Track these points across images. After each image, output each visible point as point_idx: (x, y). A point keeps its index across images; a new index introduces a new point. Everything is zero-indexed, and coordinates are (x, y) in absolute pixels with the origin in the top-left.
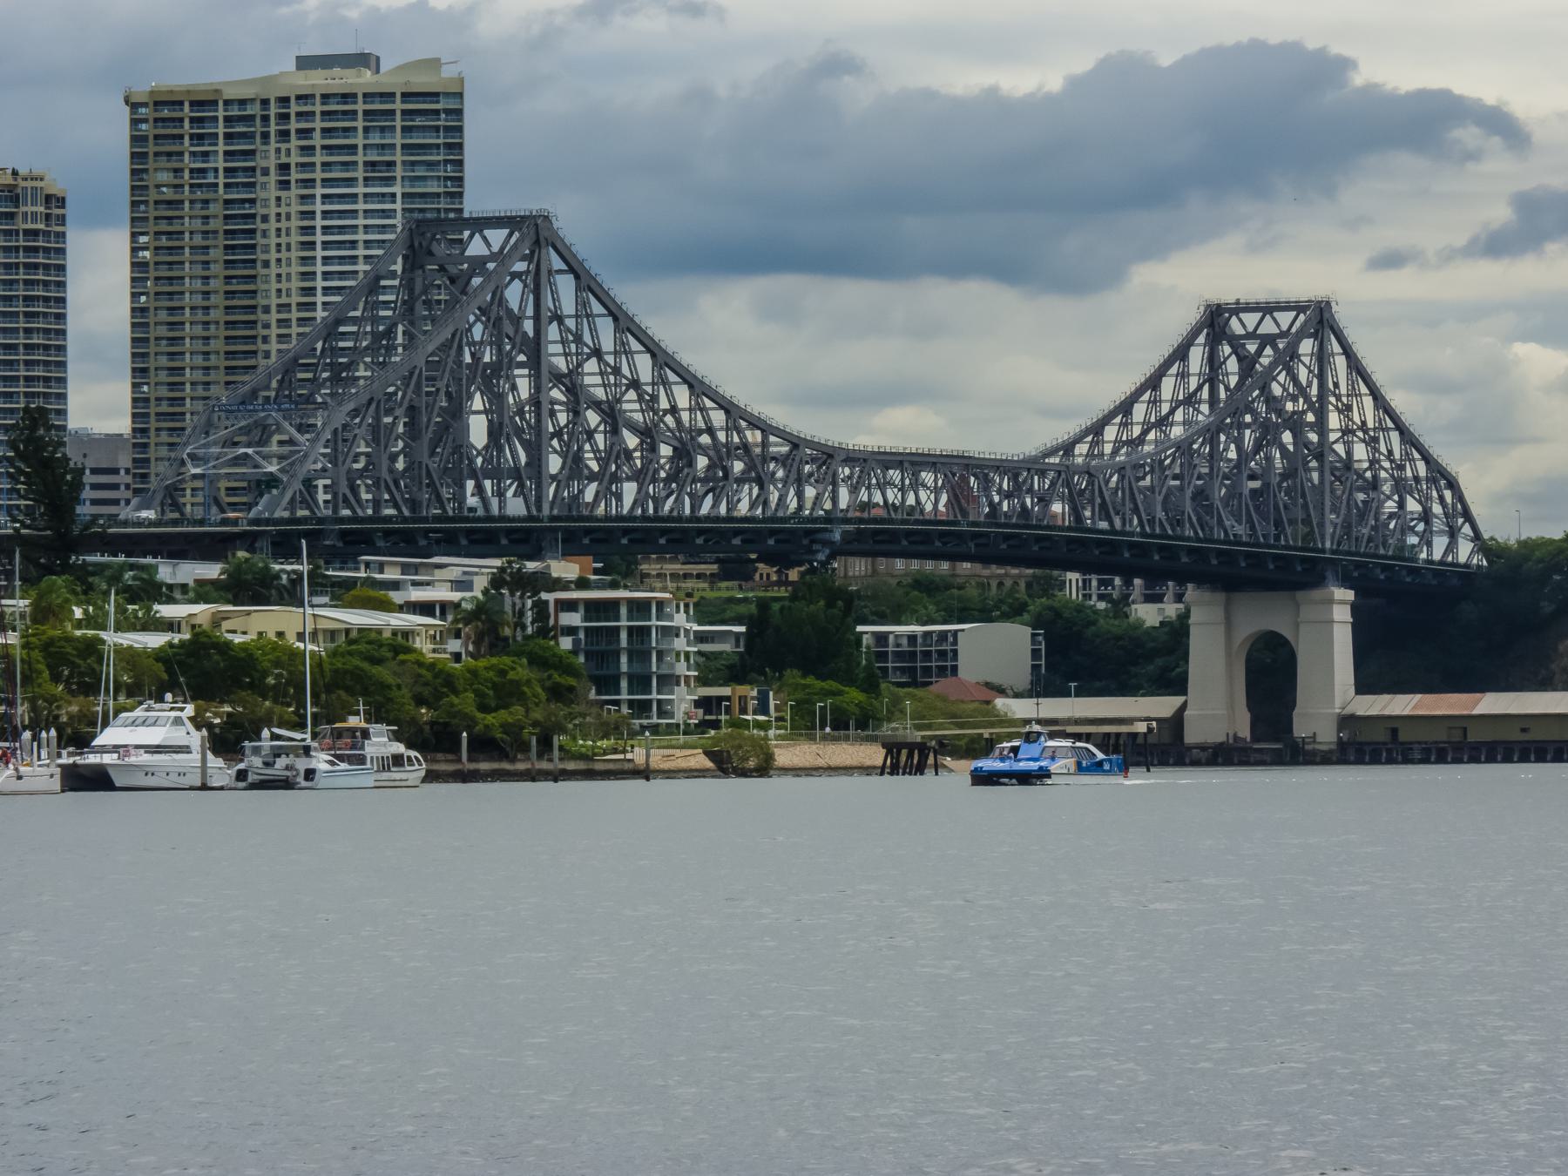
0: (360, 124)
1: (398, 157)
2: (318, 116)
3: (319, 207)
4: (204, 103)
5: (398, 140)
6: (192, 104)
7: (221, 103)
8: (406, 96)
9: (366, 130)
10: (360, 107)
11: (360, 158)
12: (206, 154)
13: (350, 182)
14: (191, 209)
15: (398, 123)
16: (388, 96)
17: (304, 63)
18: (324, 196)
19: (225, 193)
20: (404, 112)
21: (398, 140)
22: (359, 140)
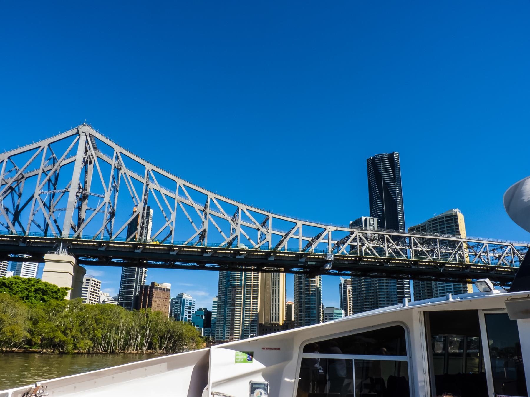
0: (438, 224)
5: (445, 226)
8: (446, 217)
15: (445, 223)
16: (443, 218)
20: (446, 220)
22: (439, 227)
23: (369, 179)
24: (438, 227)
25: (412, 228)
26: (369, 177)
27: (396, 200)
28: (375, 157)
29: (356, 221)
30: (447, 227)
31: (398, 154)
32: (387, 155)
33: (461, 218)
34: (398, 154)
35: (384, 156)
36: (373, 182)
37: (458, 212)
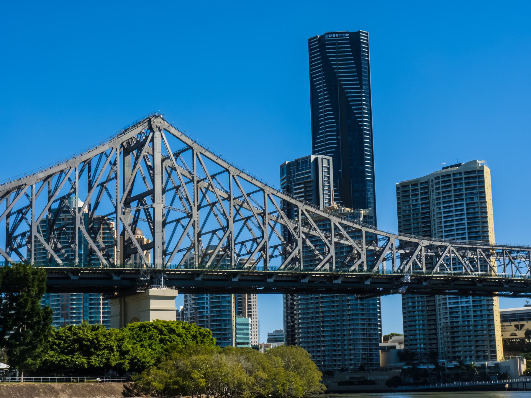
1: (464, 192)
2: (441, 183)
3: (442, 211)
4: (414, 184)
5: (464, 187)
6: (412, 185)
7: (419, 184)
8: (466, 173)
9: (455, 185)
10: (452, 178)
11: (452, 193)
12: (416, 200)
13: (451, 201)
14: (413, 217)
15: (463, 181)
16: (460, 173)
17: (444, 168)
18: (444, 207)
19: (422, 211)
20: (465, 178)
21: (464, 187)
22: (452, 188)
23: (312, 79)
24: (451, 187)
25: (403, 185)
26: (311, 75)
27: (361, 121)
28: (327, 36)
29: (296, 160)
30: (466, 189)
31: (367, 34)
32: (348, 35)
33: (487, 173)
34: (367, 34)
35: (342, 37)
36: (320, 84)
37: (484, 166)
